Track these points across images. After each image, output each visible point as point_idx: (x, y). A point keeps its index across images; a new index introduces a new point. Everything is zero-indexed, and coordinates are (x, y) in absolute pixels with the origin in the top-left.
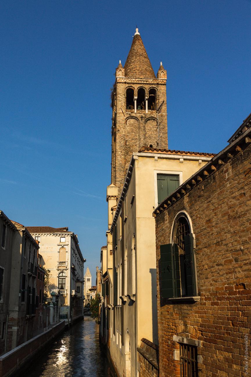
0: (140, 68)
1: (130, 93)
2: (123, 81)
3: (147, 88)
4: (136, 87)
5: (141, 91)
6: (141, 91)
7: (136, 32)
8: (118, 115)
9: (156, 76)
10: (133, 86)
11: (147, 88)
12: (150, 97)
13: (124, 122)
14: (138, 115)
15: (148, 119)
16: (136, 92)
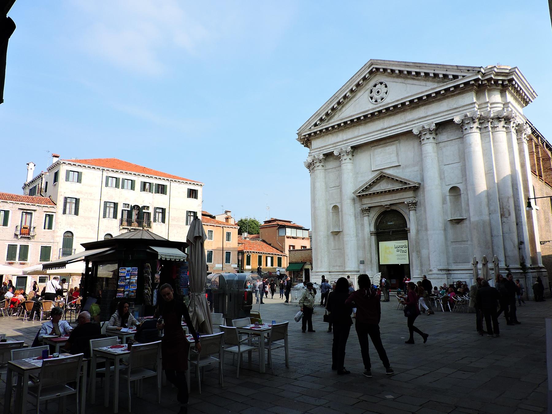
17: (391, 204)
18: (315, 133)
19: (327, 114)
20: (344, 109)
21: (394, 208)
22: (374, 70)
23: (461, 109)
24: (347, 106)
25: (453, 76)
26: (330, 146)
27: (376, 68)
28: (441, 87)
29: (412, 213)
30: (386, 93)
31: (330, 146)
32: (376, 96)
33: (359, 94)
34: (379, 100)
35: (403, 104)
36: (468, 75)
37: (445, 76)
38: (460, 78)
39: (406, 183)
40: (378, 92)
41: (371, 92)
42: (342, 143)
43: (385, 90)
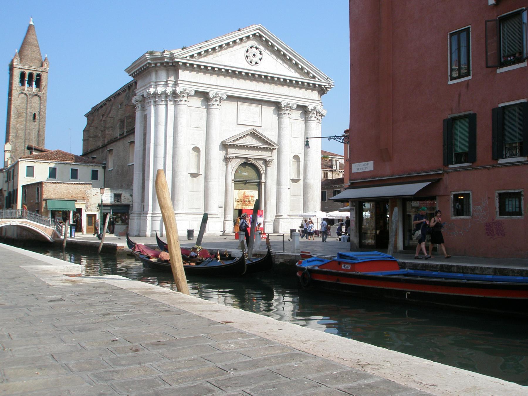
0: (31, 56)
1: (23, 75)
2: (18, 67)
3: (35, 73)
4: (27, 72)
5: (31, 75)
6: (31, 75)
7: (30, 20)
8: (13, 91)
9: (42, 66)
10: (25, 71)
11: (35, 73)
12: (37, 79)
13: (17, 96)
14: (27, 93)
15: (35, 96)
16: (27, 76)
17: (254, 159)
18: (192, 65)
19: (206, 51)
20: (220, 53)
21: (253, 161)
22: (257, 34)
23: (311, 101)
24: (223, 52)
25: (313, 75)
26: (203, 85)
27: (259, 34)
28: (306, 81)
29: (268, 169)
30: (260, 60)
31: (203, 85)
32: (251, 58)
33: (236, 47)
34: (254, 63)
35: (279, 79)
36: (323, 81)
37: (308, 73)
38: (317, 80)
39: (270, 144)
40: (254, 55)
41: (247, 51)
42: (216, 87)
43: (260, 56)
